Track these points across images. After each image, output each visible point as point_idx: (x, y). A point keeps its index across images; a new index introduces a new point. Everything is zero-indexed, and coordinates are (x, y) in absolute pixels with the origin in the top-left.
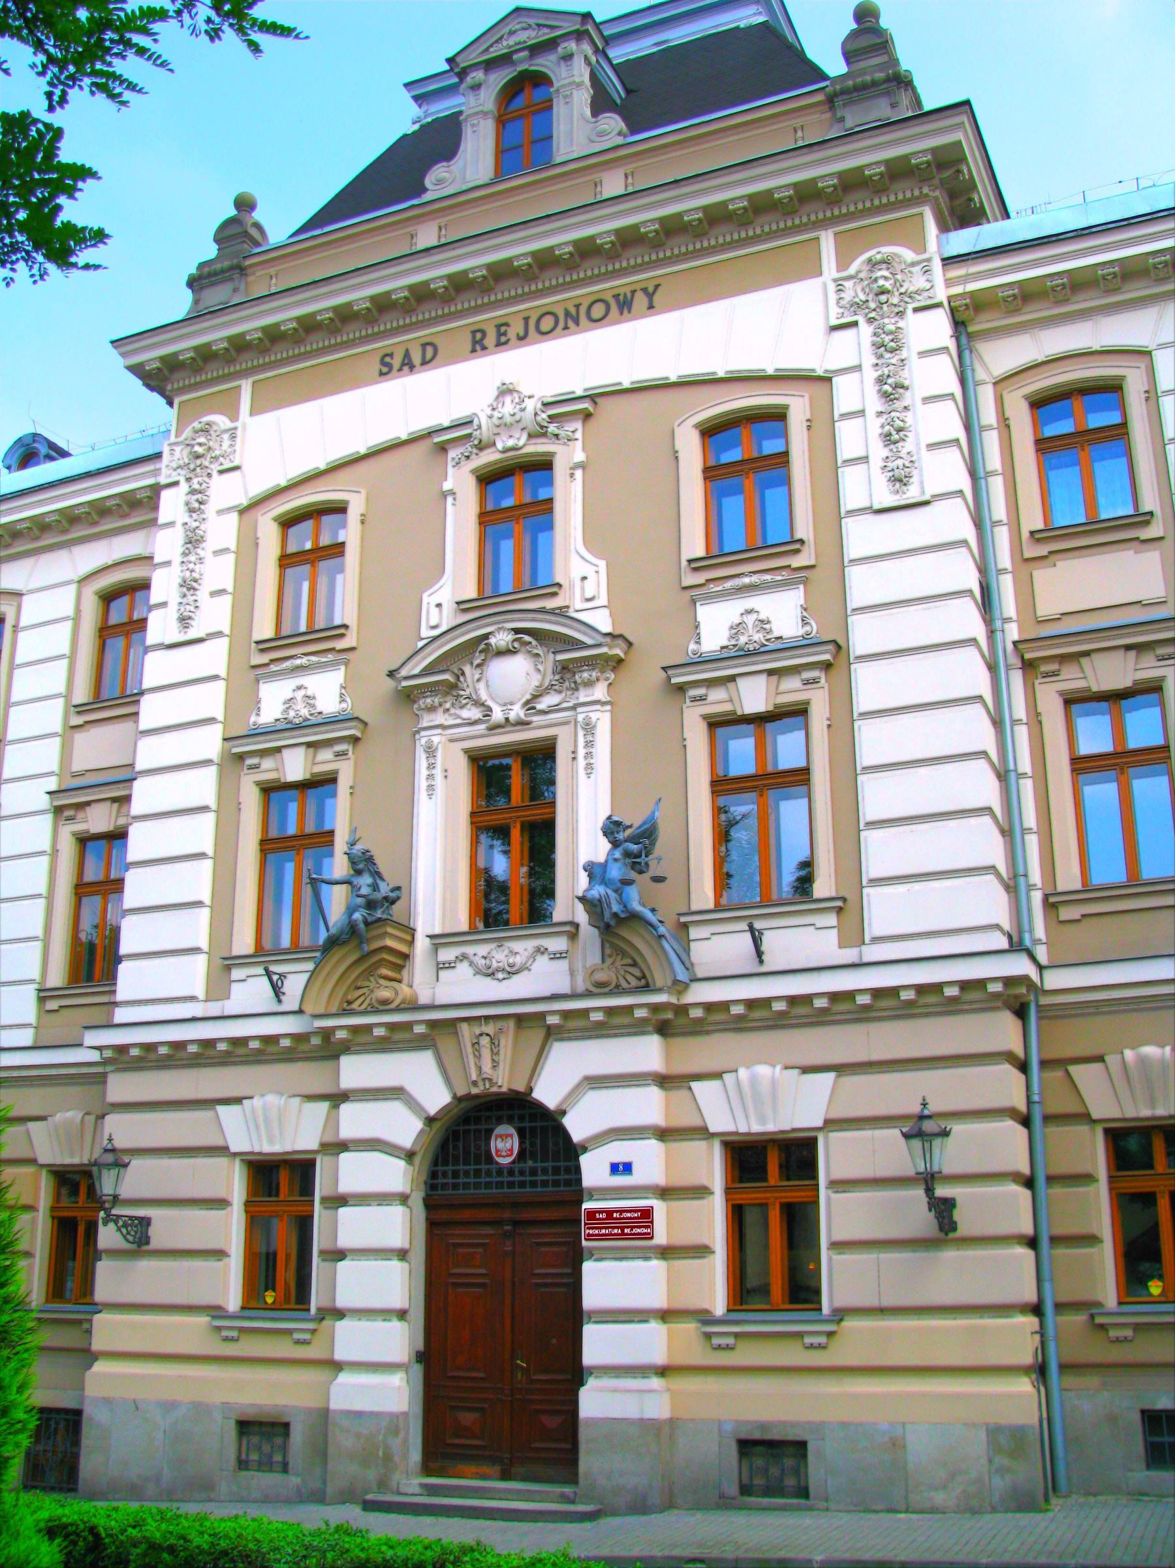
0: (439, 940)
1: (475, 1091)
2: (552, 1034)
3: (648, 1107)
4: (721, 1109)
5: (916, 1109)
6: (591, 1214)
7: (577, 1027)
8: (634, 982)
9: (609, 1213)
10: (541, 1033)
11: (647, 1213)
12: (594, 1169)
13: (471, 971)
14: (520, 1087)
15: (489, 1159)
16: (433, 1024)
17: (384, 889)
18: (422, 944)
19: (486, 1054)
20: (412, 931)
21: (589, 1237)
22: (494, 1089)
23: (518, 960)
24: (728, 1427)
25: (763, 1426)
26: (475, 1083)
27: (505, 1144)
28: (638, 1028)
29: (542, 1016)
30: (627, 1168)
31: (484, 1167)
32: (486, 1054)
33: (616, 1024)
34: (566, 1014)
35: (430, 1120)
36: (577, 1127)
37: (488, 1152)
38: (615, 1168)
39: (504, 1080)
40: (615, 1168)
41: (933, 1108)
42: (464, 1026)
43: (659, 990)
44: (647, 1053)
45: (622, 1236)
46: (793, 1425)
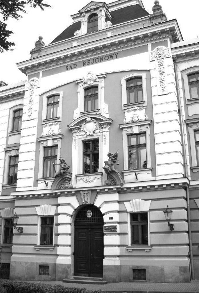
0: (77, 176)
1: (84, 204)
9: (109, 227)
10: (96, 193)
11: (116, 227)
12: (106, 219)
13: (83, 181)
14: (92, 203)
16: (76, 191)
19: (86, 197)
23: (92, 179)
26: (84, 203)
30: (112, 218)
32: (86, 197)
36: (103, 211)
38: (110, 218)
39: (89, 202)
40: (110, 218)
42: (82, 192)
45: (111, 231)
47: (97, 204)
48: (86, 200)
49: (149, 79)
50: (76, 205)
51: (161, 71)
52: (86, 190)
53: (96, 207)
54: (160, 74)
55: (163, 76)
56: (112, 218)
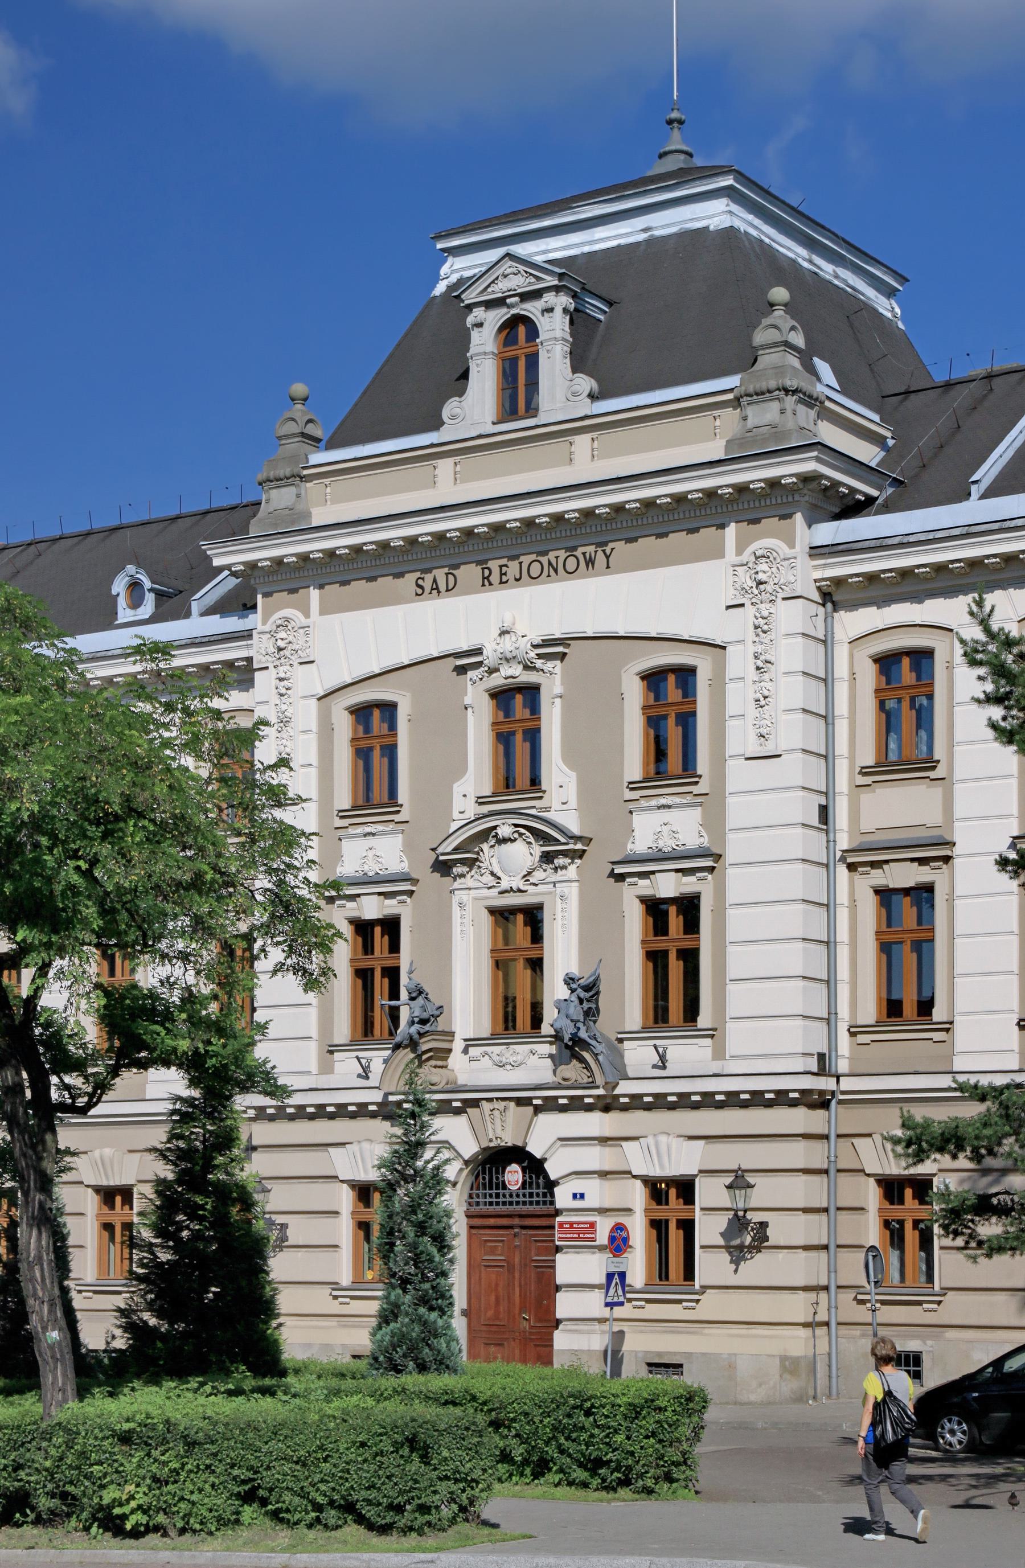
0: (470, 1043)
1: (492, 1145)
2: (537, 1110)
3: (593, 1158)
4: (639, 1159)
5: (736, 1167)
6: (561, 1225)
7: (551, 1105)
8: (586, 1080)
9: (571, 1224)
10: (531, 1109)
11: (592, 1225)
12: (562, 1197)
13: (490, 1063)
14: (520, 1144)
15: (505, 1187)
16: (464, 1101)
17: (431, 1010)
18: (458, 1045)
19: (498, 1122)
20: (452, 1034)
21: (561, 1239)
22: (503, 1144)
23: (519, 1058)
24: (640, 1355)
25: (659, 1354)
26: (491, 1140)
27: (514, 1175)
28: (589, 1108)
29: (531, 1099)
30: (582, 1196)
31: (501, 1191)
32: (498, 1122)
33: (576, 1105)
34: (545, 1099)
35: (467, 1163)
36: (553, 1170)
37: (504, 1182)
38: (575, 1196)
39: (509, 1139)
41: (743, 1167)
42: (484, 1103)
43: (598, 1087)
44: (594, 1123)
45: (579, 1239)
46: (675, 1354)
47: (536, 1149)
48: (499, 1133)
49: (719, 683)
50: (469, 1148)
51: (762, 658)
52: (497, 1099)
53: (530, 1156)
54: (758, 668)
55: (766, 676)
56: (582, 1196)
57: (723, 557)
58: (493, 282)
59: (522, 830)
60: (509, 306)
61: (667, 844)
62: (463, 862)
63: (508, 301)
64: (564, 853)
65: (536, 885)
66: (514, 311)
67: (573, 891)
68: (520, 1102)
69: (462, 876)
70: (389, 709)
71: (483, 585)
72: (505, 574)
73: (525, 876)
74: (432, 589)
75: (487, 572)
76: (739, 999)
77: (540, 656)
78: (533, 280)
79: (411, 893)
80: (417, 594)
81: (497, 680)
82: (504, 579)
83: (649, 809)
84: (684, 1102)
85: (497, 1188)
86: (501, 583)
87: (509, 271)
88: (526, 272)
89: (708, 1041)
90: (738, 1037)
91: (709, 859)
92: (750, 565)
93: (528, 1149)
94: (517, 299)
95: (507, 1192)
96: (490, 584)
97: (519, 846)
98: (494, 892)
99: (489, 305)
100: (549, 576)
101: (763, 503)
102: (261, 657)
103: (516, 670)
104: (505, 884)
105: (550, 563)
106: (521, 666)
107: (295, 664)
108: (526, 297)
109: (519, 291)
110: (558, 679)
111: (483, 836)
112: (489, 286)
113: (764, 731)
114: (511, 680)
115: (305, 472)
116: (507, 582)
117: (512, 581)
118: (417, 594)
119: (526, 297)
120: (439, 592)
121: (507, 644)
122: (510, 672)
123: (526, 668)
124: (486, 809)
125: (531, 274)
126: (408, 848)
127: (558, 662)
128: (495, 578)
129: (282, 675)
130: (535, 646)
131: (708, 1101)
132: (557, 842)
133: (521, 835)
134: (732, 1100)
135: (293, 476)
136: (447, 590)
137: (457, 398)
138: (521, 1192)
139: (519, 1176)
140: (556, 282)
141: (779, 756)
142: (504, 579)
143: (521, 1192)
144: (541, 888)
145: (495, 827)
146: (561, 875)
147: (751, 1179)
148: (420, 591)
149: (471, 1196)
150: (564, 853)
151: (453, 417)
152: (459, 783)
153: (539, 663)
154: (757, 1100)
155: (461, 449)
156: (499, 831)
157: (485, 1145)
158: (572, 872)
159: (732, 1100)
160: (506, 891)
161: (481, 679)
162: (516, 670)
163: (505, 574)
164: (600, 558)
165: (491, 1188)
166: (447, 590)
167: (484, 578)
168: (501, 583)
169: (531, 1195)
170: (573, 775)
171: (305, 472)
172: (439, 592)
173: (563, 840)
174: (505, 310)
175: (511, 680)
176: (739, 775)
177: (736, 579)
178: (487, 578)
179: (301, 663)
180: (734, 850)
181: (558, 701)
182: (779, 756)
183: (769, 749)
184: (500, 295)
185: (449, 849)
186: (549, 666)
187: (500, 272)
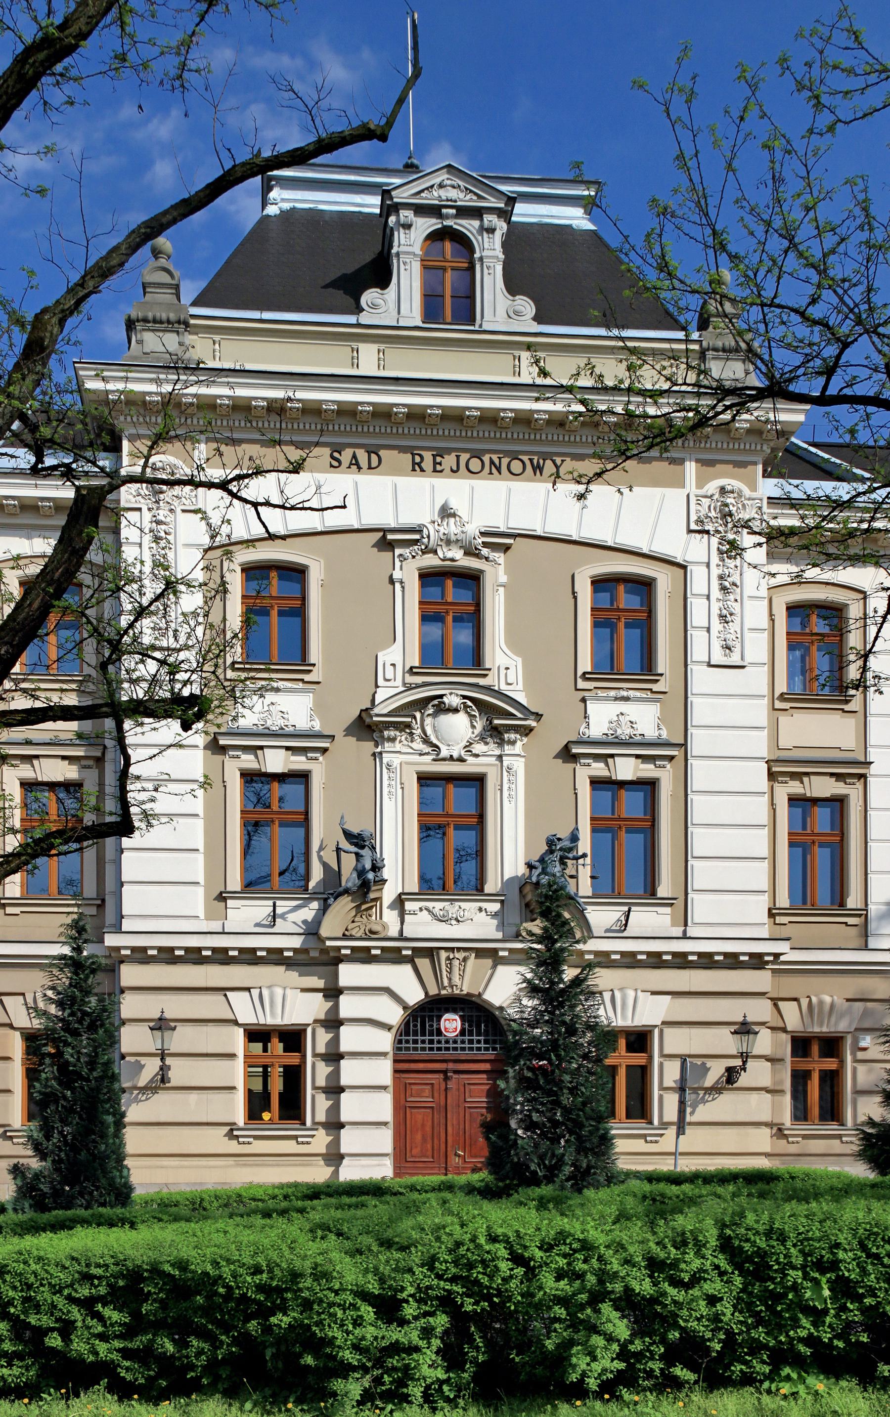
15: (439, 1033)
31: (436, 1038)
50: (414, 995)
55: (732, 597)
57: (683, 486)
58: (427, 189)
59: (469, 703)
60: (440, 216)
61: (624, 732)
62: (397, 726)
63: (444, 211)
64: (516, 729)
65: (477, 756)
66: (448, 223)
67: (519, 766)
68: (480, 953)
69: (393, 740)
70: (296, 573)
71: (414, 470)
72: (440, 464)
73: (466, 747)
74: (351, 464)
75: (418, 459)
76: (702, 874)
77: (485, 545)
78: (475, 198)
79: (324, 750)
80: (332, 466)
81: (430, 561)
82: (438, 468)
83: (607, 699)
84: (656, 961)
85: (431, 1034)
86: (435, 471)
87: (449, 182)
88: (467, 189)
89: (668, 910)
90: (702, 908)
91: (675, 750)
92: (715, 498)
93: (486, 996)
94: (454, 211)
95: (442, 1038)
96: (422, 470)
97: (461, 719)
98: (428, 759)
99: (421, 210)
100: (491, 473)
101: (731, 446)
102: (131, 497)
103: (457, 554)
104: (444, 753)
105: (492, 462)
106: (462, 552)
107: (178, 510)
108: (464, 212)
109: (459, 203)
110: (501, 569)
111: (422, 704)
112: (422, 191)
113: (730, 643)
114: (448, 563)
115: (192, 322)
116: (441, 471)
117: (447, 470)
118: (332, 466)
119: (464, 212)
120: (359, 468)
121: (452, 528)
122: (449, 555)
123: (466, 554)
124: (419, 680)
125: (471, 191)
126: (318, 709)
127: (502, 555)
128: (428, 464)
129: (161, 518)
130: (483, 534)
131: (681, 961)
132: (511, 716)
133: (466, 706)
134: (707, 961)
135: (179, 322)
136: (370, 468)
137: (378, 290)
138: (460, 1038)
139: (458, 1024)
140: (502, 205)
141: (743, 667)
142: (438, 468)
143: (460, 1038)
144: (481, 760)
145: (441, 696)
146: (508, 749)
147: (756, 1028)
148: (335, 464)
149: (400, 1042)
150: (516, 729)
151: (374, 306)
152: (385, 652)
153: (485, 551)
154: (732, 961)
155: (391, 337)
156: (445, 699)
157: (433, 991)
158: (518, 748)
159: (707, 961)
160: (444, 759)
161: (414, 557)
162: (457, 554)
163: (440, 464)
164: (549, 467)
165: (423, 1034)
166: (370, 468)
167: (414, 463)
168: (435, 471)
169: (471, 1042)
170: (519, 660)
171: (192, 322)
172: (359, 468)
173: (519, 715)
174: (434, 221)
175: (448, 563)
176: (701, 679)
177: (699, 508)
178: (419, 464)
179: (183, 511)
180: (699, 742)
181: (501, 589)
182: (743, 667)
183: (735, 659)
184: (437, 202)
185: (385, 711)
186: (494, 555)
187: (438, 180)
